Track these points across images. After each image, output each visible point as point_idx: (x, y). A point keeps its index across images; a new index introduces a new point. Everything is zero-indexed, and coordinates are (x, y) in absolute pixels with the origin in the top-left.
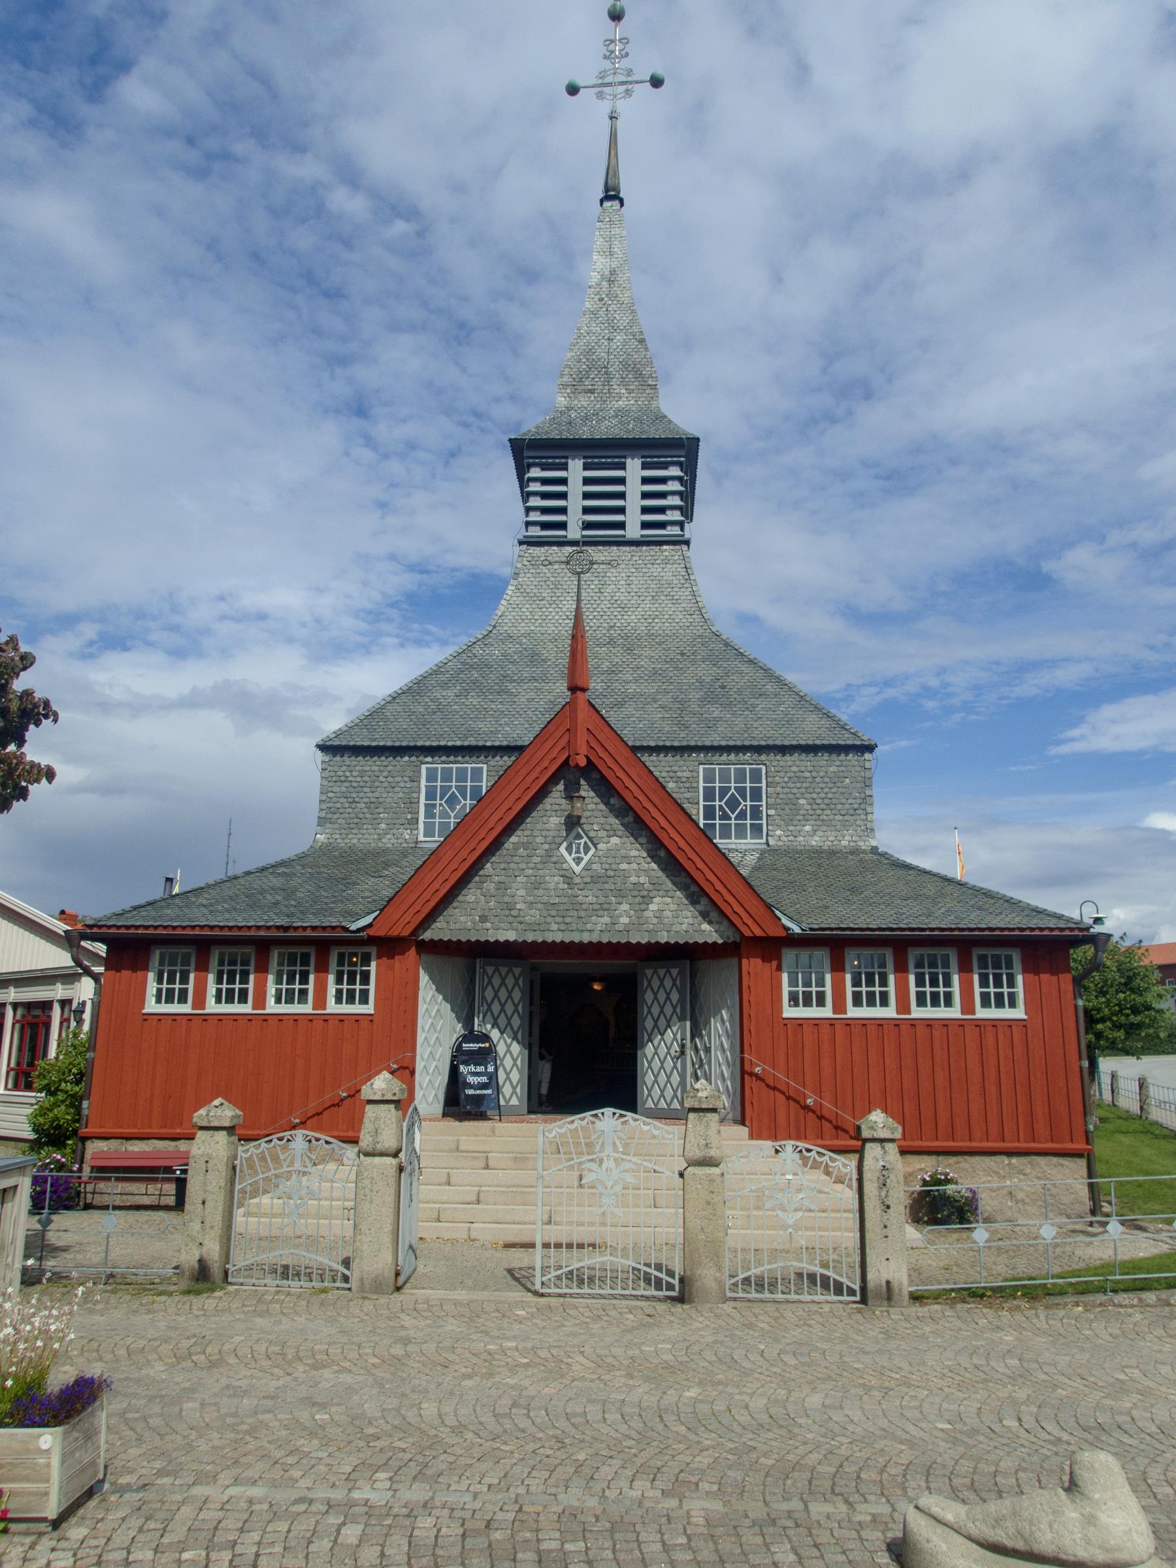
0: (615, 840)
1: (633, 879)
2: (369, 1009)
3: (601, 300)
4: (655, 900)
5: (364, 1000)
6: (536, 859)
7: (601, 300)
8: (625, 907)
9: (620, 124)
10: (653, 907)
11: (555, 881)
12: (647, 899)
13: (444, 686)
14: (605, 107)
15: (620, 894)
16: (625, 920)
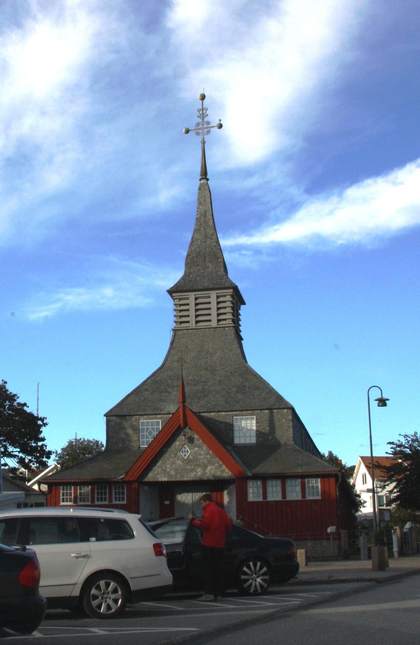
0: (196, 449)
1: (202, 461)
2: (125, 502)
3: (201, 224)
4: (209, 467)
5: (123, 500)
6: (172, 455)
7: (201, 224)
8: (199, 469)
9: (205, 145)
10: (208, 469)
11: (179, 462)
12: (205, 467)
13: (146, 390)
14: (200, 138)
15: (199, 465)
16: (199, 473)
